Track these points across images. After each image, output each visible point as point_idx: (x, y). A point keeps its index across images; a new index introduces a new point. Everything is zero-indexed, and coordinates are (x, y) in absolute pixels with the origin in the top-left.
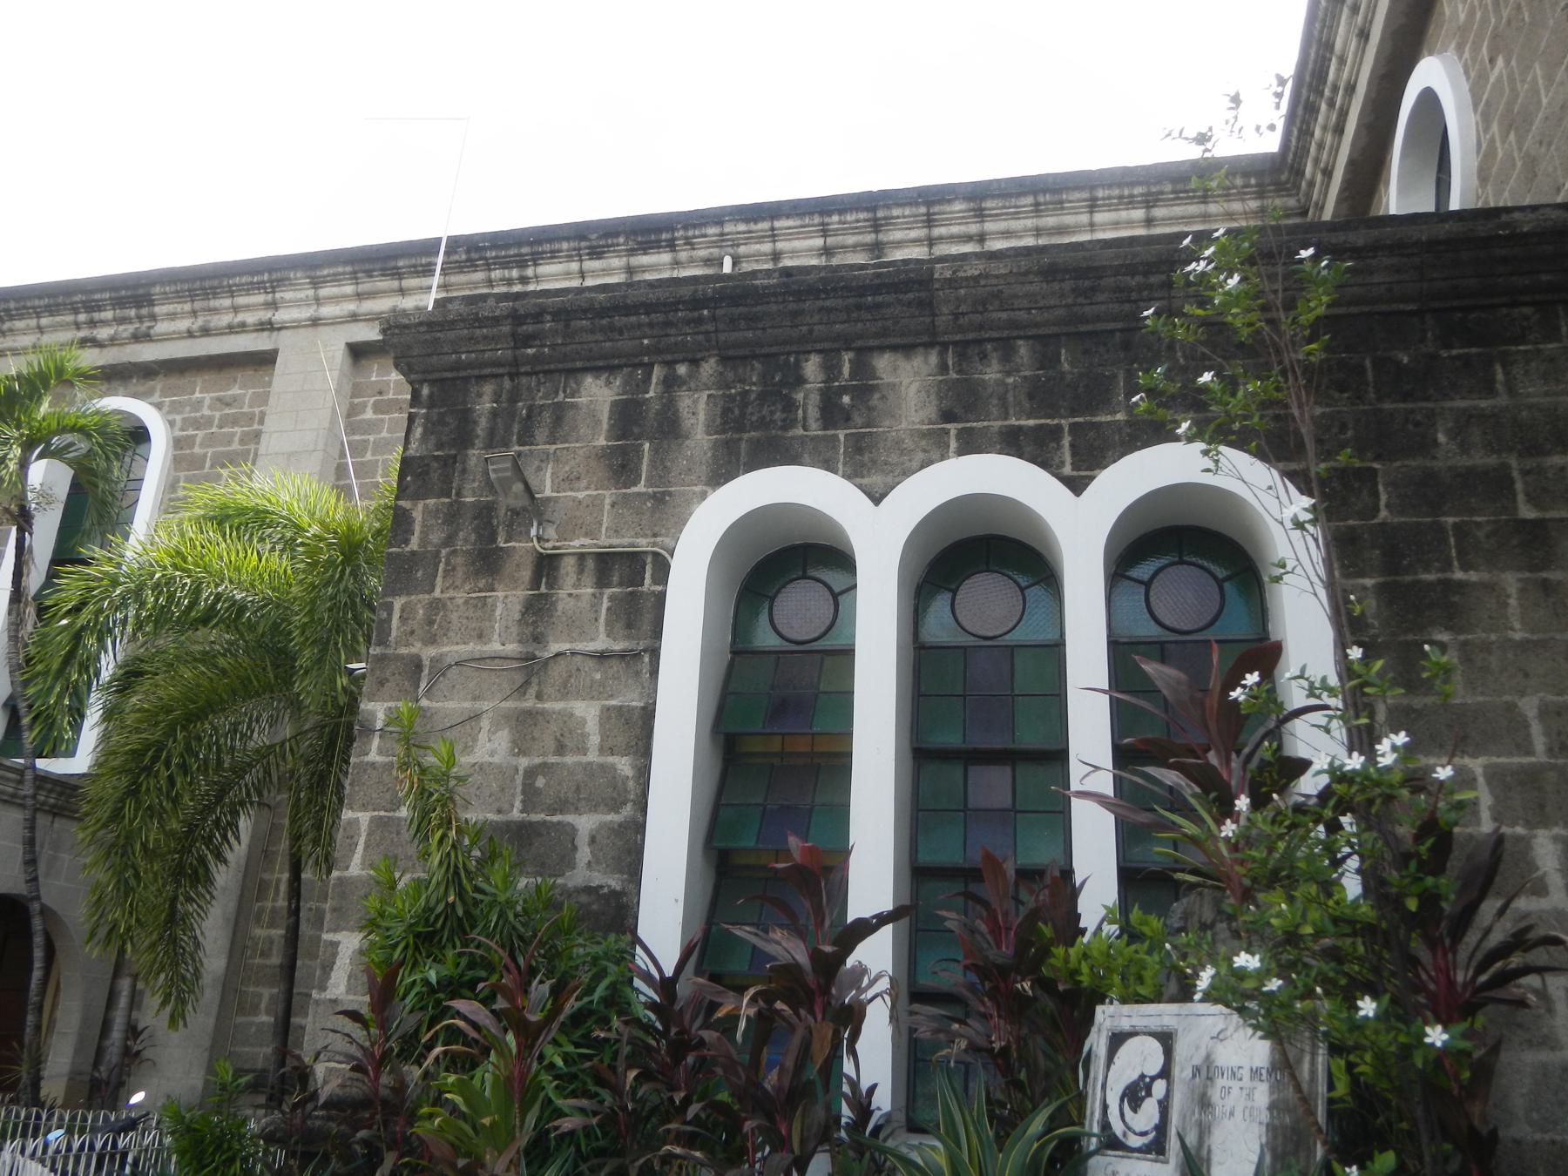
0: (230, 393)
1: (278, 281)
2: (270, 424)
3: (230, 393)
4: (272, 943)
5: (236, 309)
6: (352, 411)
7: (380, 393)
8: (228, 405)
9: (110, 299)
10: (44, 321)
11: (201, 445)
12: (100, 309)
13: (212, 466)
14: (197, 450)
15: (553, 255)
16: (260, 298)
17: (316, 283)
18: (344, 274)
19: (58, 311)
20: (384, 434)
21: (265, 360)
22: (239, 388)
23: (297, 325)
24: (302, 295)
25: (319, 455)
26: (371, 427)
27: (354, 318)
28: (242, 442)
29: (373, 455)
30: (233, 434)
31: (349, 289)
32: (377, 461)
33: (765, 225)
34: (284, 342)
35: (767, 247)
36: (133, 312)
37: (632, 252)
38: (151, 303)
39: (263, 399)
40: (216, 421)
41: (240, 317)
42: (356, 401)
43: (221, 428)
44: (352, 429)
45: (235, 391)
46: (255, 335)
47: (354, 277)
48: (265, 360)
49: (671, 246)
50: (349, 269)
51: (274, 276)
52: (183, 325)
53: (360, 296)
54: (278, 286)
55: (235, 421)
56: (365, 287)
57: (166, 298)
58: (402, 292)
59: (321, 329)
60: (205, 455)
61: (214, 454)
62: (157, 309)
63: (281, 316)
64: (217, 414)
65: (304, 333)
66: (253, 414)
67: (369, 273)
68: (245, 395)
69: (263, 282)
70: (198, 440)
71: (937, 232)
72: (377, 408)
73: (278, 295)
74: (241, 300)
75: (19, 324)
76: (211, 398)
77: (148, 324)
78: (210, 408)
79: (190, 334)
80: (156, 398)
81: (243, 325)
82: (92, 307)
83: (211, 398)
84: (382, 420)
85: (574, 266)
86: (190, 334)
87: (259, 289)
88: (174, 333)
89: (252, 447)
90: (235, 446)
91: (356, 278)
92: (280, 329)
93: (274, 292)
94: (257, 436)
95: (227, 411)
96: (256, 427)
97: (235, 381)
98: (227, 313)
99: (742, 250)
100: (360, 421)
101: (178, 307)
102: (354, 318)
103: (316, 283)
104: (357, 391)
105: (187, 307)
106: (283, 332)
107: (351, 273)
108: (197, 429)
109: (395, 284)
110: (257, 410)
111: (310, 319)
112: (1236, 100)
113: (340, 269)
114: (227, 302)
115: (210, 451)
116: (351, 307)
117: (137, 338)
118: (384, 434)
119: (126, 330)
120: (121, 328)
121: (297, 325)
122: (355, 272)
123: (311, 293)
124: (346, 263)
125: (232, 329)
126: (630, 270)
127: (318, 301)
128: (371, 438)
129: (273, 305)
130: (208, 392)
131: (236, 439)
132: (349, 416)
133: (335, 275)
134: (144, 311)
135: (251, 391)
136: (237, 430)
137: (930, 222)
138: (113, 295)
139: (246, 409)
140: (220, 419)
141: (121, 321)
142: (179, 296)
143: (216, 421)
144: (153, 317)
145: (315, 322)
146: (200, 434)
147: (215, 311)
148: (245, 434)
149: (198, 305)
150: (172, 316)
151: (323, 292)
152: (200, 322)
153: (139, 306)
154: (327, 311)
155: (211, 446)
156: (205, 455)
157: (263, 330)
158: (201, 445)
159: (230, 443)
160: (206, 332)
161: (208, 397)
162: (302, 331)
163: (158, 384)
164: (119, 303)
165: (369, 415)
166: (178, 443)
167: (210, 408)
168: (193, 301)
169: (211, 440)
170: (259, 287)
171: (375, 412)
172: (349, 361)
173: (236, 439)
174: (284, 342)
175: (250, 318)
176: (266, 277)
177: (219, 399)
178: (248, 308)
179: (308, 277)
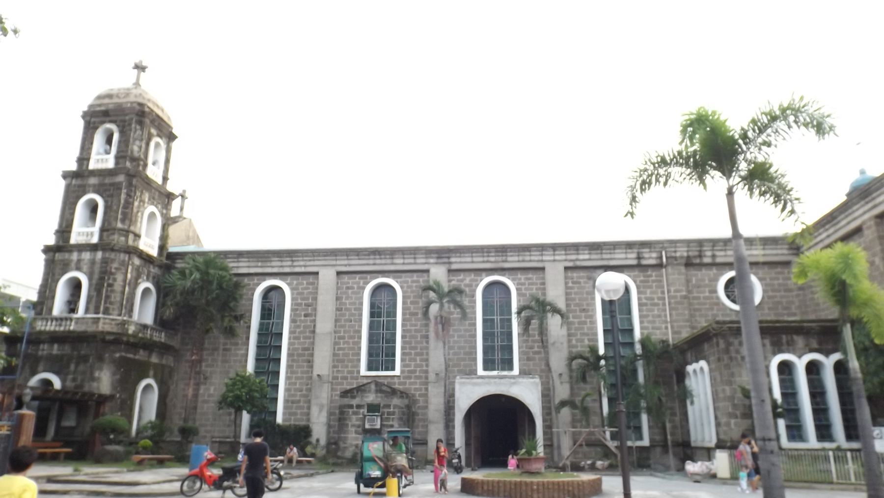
10: (474, 255)
12: (490, 252)
15: (620, 249)
17: (554, 250)
21: (543, 269)
23: (549, 261)
26: (571, 288)
27: (566, 260)
33: (674, 245)
34: (547, 266)
35: (673, 249)
37: (639, 248)
49: (650, 248)
53: (566, 254)
56: (568, 252)
63: (545, 258)
67: (570, 250)
71: (715, 248)
74: (532, 253)
75: (467, 255)
79: (519, 261)
80: (507, 276)
85: (624, 251)
86: (519, 261)
99: (667, 250)
102: (566, 260)
105: (517, 254)
112: (783, 220)
114: (528, 253)
117: (503, 261)
119: (500, 259)
125: (531, 261)
126: (638, 253)
137: (713, 246)
145: (554, 261)
154: (557, 258)
160: (523, 261)
161: (523, 277)
163: (507, 273)
164: (497, 252)
166: (517, 289)
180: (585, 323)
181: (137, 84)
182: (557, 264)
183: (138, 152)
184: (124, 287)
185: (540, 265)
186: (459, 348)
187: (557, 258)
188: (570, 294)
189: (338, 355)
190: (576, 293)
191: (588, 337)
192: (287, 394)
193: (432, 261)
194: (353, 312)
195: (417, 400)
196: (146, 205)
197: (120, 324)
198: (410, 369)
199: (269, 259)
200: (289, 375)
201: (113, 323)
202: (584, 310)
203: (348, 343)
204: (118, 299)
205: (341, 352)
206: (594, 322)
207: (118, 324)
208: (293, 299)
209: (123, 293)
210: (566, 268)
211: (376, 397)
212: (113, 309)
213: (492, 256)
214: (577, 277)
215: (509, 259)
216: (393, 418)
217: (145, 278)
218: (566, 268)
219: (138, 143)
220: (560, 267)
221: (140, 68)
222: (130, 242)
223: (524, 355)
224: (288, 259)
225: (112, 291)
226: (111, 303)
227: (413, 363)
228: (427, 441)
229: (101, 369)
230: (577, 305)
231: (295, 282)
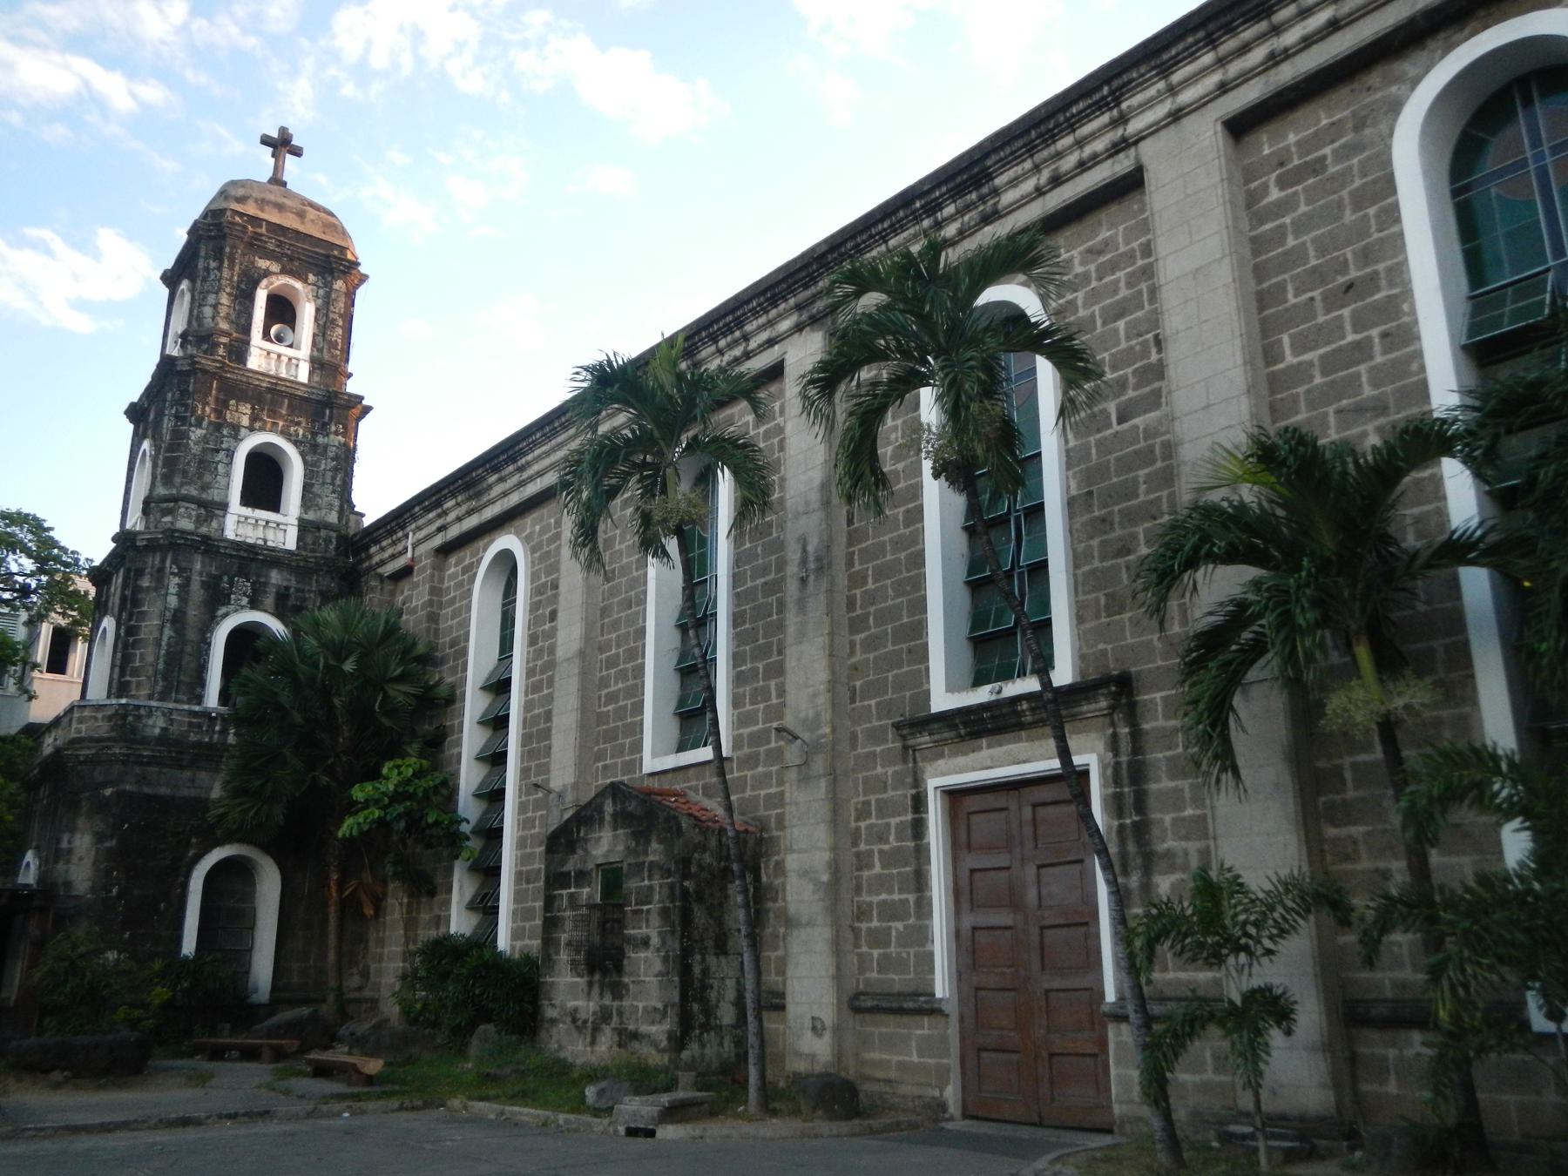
0: (1099, 238)
1: (1119, 88)
2: (1163, 247)
3: (1099, 238)
4: (1355, 843)
5: (1080, 144)
6: (1252, 199)
7: (1281, 164)
8: (1100, 252)
9: (948, 191)
11: (1085, 306)
12: (940, 207)
13: (1104, 324)
14: (1082, 313)
16: (1105, 118)
18: (1197, 42)
19: (901, 227)
20: (1303, 208)
21: (1132, 183)
22: (1109, 229)
23: (1155, 129)
24: (1152, 92)
25: (1227, 261)
27: (1224, 88)
28: (1129, 285)
29: (1296, 238)
30: (1118, 281)
31: (1207, 59)
32: (1304, 243)
36: (974, 196)
38: (990, 178)
39: (1145, 227)
40: (1094, 275)
41: (1088, 151)
42: (1253, 186)
43: (1100, 279)
44: (1259, 218)
45: (1105, 234)
46: (1110, 162)
47: (1211, 42)
48: (1132, 183)
50: (1201, 34)
51: (1115, 84)
52: (1028, 186)
53: (1221, 62)
54: (1122, 95)
55: (1113, 266)
56: (1230, 44)
57: (1005, 164)
58: (1276, 30)
59: (1185, 121)
60: (1093, 316)
61: (1102, 309)
62: (997, 182)
63: (1134, 126)
64: (1092, 267)
65: (1167, 136)
66: (1133, 251)
67: (1230, 30)
68: (1117, 234)
69: (1104, 98)
70: (1080, 303)
72: (1283, 183)
73: (1124, 106)
76: (1080, 253)
77: (991, 203)
78: (1082, 263)
79: (1039, 192)
81: (1095, 156)
82: (933, 208)
83: (1080, 253)
84: (1295, 194)
86: (1039, 192)
87: (1100, 108)
88: (1023, 197)
89: (1144, 286)
90: (1124, 292)
91: (1213, 41)
92: (1136, 143)
93: (1118, 104)
94: (1148, 272)
95: (1102, 259)
96: (1140, 263)
97: (1100, 223)
98: (1071, 153)
100: (1265, 206)
101: (1018, 170)
102: (1224, 88)
103: (1165, 71)
104: (1249, 175)
105: (1028, 165)
106: (1142, 145)
107: (1205, 38)
108: (1075, 291)
109: (1263, 26)
110: (1135, 245)
111: (1170, 114)
113: (1190, 40)
114: (1068, 141)
115: (1096, 308)
116: (1214, 79)
117: (987, 219)
118: (1303, 208)
120: (966, 218)
121: (1155, 129)
122: (1209, 35)
123: (1161, 85)
124: (1194, 30)
125: (1083, 166)
127: (1172, 91)
128: (1288, 220)
129: (1122, 120)
130: (1074, 248)
131: (1122, 284)
132: (1249, 206)
133: (1186, 49)
134: (985, 190)
135: (1121, 228)
136: (1120, 274)
138: (951, 185)
139: (1122, 249)
140: (1097, 270)
141: (960, 213)
142: (1015, 159)
143: (1094, 275)
144: (996, 192)
145: (1176, 116)
146: (1080, 295)
147: (1059, 155)
148: (1130, 276)
149: (1038, 157)
150: (1014, 182)
151: (1176, 77)
152: (1045, 175)
153: (978, 186)
154: (1187, 96)
155: (1096, 303)
156: (1093, 316)
157: (1117, 152)
158: (1085, 306)
159: (1116, 292)
160: (1057, 181)
162: (1163, 133)
164: (957, 193)
165: (1275, 194)
167: (1082, 263)
168: (1032, 156)
169: (1093, 297)
170: (1101, 106)
171: (1282, 189)
172: (1230, 141)
173: (1122, 284)
174: (1147, 149)
175: (1099, 145)
176: (1106, 90)
177: (1090, 251)
178: (1093, 136)
179: (1153, 69)
180: (1361, 350)
181: (277, 180)
182: (1188, 123)
183: (213, 318)
184: (162, 627)
185: (1121, 165)
186: (881, 618)
187: (1187, 96)
188: (1280, 235)
189: (602, 718)
190: (1300, 227)
191: (1382, 421)
192: (519, 853)
193: (785, 325)
194: (635, 574)
195: (771, 838)
196: (243, 432)
197: (116, 714)
198: (755, 728)
199: (485, 485)
200: (524, 798)
201: (100, 715)
202: (1350, 287)
203: (622, 675)
204: (150, 659)
205: (610, 708)
206: (1405, 336)
207: (110, 718)
208: (534, 576)
209: (158, 643)
210: (1240, 127)
211: (615, 837)
212: (139, 684)
213: (951, 219)
214: (1299, 144)
215: (1008, 198)
216: (648, 911)
217: (245, 601)
218: (1240, 127)
219: (211, 299)
220: (1206, 130)
221: (281, 144)
222: (185, 524)
223: (1095, 589)
224: (511, 468)
225: (135, 645)
226: (135, 672)
227: (762, 706)
228: (782, 995)
229: (73, 830)
230: (1318, 276)
231: (537, 528)
